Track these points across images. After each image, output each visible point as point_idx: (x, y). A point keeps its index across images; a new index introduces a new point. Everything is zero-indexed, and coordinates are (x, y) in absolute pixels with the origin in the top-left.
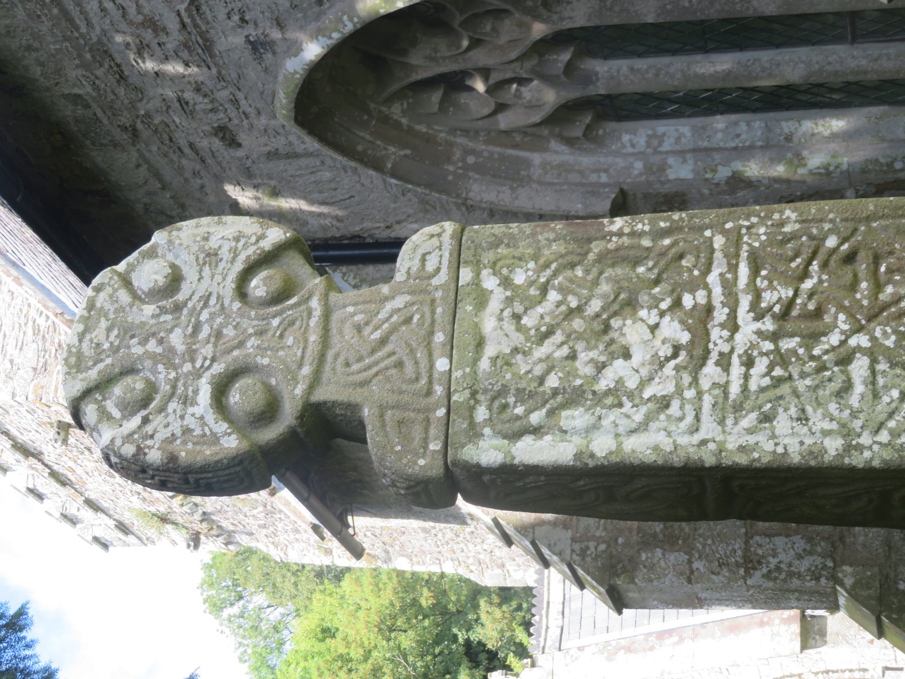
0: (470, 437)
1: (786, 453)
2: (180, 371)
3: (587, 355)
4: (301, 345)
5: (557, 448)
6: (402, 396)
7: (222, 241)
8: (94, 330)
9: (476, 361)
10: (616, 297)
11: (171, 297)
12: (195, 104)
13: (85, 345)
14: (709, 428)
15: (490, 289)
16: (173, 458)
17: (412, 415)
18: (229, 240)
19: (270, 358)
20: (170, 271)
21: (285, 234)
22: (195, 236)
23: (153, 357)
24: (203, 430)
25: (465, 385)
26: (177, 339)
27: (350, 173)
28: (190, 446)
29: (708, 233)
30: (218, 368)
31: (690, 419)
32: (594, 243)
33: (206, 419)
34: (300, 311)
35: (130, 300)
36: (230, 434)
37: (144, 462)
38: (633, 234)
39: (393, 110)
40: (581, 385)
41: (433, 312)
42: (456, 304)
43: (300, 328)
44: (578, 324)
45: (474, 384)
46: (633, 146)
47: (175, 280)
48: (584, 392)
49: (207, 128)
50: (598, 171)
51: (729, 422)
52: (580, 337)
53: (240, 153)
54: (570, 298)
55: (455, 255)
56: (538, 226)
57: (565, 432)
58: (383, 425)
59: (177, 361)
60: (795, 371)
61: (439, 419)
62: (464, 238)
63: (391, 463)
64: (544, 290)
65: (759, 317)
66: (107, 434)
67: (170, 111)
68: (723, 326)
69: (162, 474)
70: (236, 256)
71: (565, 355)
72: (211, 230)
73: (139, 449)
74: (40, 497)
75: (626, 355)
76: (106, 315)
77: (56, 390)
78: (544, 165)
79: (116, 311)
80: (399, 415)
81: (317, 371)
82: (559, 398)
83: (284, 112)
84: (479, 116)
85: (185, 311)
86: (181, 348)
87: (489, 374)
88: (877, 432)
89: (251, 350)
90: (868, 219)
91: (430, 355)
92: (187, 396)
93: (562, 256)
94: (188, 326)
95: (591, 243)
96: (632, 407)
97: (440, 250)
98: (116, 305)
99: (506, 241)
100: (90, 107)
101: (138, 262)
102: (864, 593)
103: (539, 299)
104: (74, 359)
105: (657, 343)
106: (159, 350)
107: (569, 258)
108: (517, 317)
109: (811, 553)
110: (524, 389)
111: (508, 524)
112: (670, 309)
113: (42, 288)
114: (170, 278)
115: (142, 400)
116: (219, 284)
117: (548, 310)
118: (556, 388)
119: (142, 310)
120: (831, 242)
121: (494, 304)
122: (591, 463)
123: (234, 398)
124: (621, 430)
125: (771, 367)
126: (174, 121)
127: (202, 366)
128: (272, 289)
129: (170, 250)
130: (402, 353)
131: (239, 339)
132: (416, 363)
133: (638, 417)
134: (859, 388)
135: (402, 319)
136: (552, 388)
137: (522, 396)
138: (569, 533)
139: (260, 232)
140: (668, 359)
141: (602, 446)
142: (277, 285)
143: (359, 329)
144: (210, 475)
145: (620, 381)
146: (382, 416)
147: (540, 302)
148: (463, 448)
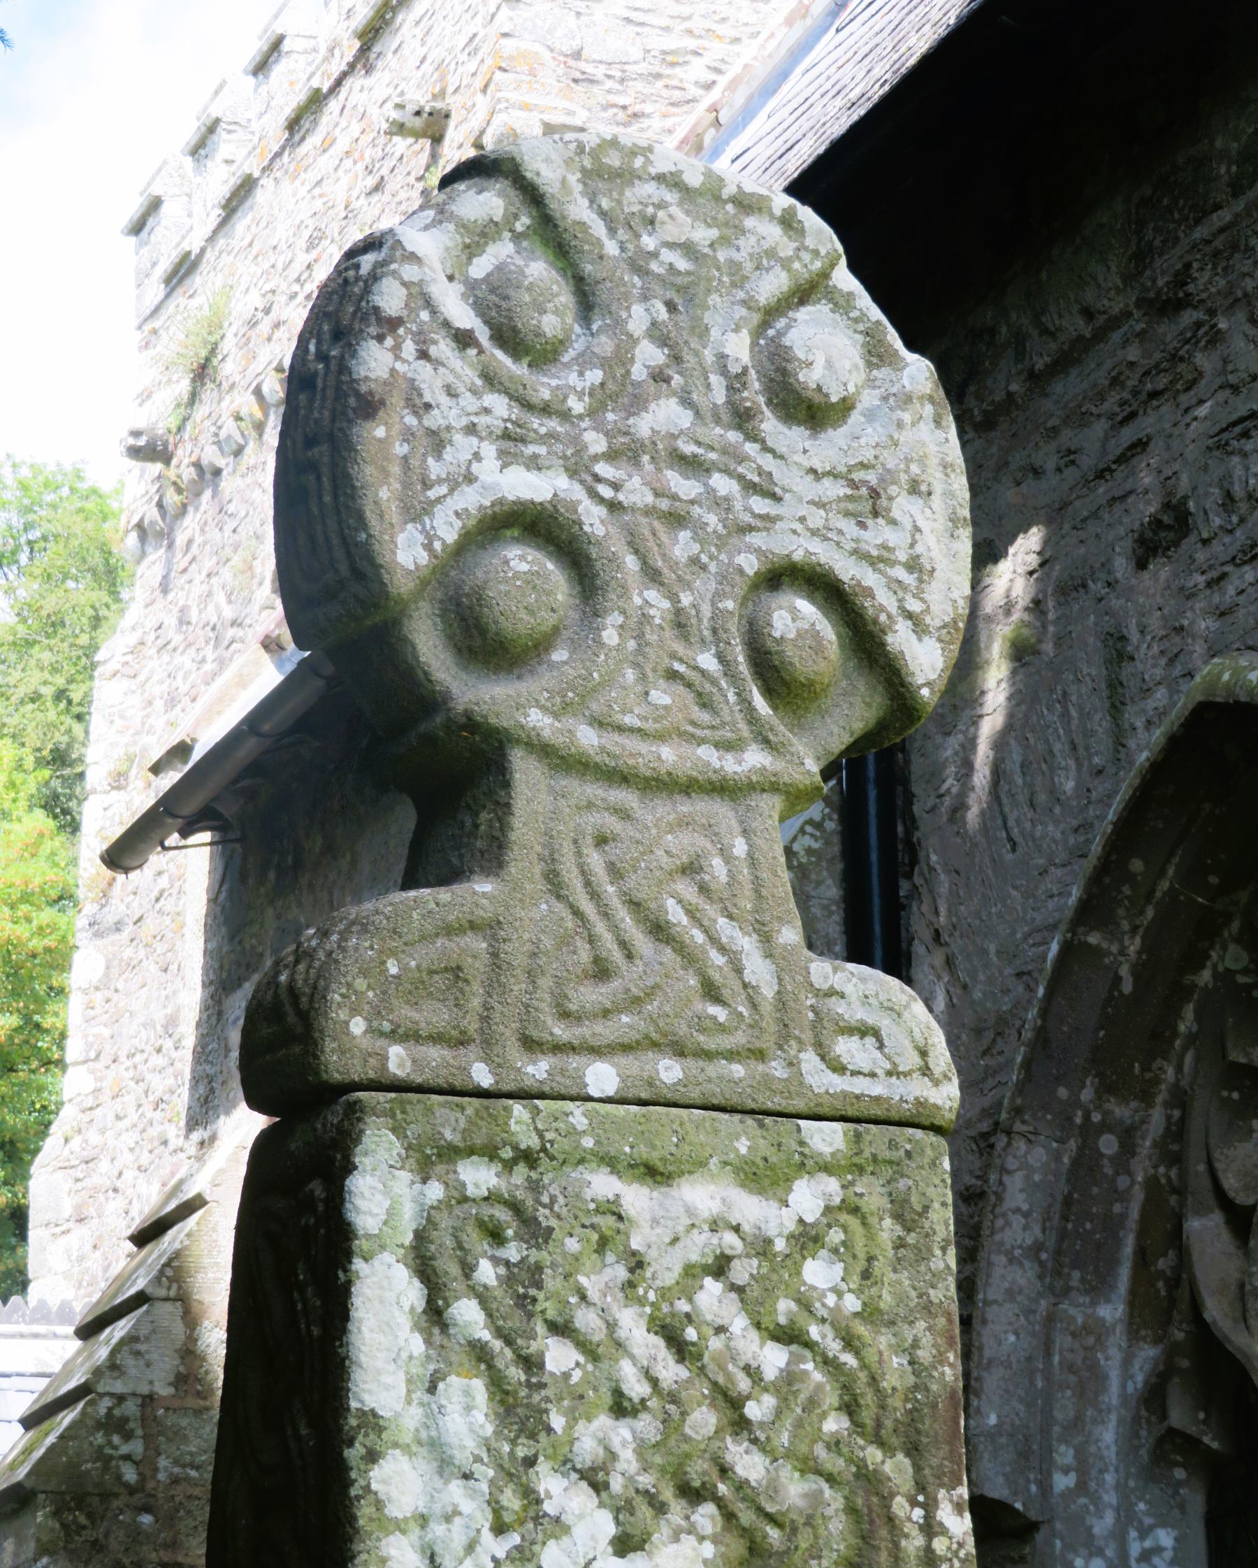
0: (420, 1149)
2: (586, 424)
3: (624, 1444)
4: (649, 726)
5: (392, 1367)
6: (523, 977)
7: (909, 526)
8: (688, 213)
9: (610, 1162)
10: (771, 1519)
11: (769, 403)
12: (1245, 455)
13: (649, 190)
15: (791, 1199)
16: (370, 407)
17: (476, 1003)
18: (912, 546)
19: (618, 648)
20: (834, 399)
21: (928, 684)
22: (922, 461)
23: (621, 359)
24: (440, 481)
25: (549, 1136)
26: (664, 416)
27: (1072, 841)
28: (400, 449)
30: (593, 519)
32: (907, 1461)
33: (466, 489)
34: (734, 723)
35: (762, 301)
36: (428, 547)
37: (360, 335)
39: (1233, 948)
40: (549, 1430)
41: (731, 1055)
42: (752, 1112)
43: (693, 723)
44: (703, 1420)
45: (552, 1158)
46: (1146, 1556)
47: (813, 413)
48: (533, 1436)
49: (1184, 484)
50: (1082, 1467)
53: (1122, 566)
54: (769, 1401)
55: (878, 1112)
56: (950, 1321)
57: (432, 1389)
58: (450, 931)
59: (610, 416)
61: (465, 1070)
62: (919, 1134)
63: (356, 949)
64: (788, 1336)
66: (430, 245)
67: (1228, 391)
69: (331, 381)
71: (625, 1389)
72: (936, 501)
73: (394, 324)
74: (261, 67)
76: (724, 241)
77: (525, 107)
78: (1095, 1331)
79: (735, 267)
80: (477, 968)
81: (586, 765)
82: (516, 1374)
83: (1226, 677)
84: (1217, 1165)
85: (733, 436)
86: (644, 425)
87: (578, 1196)
89: (638, 601)
92: (523, 440)
93: (874, 1380)
94: (699, 444)
95: (908, 1454)
96: (494, 1559)
97: (889, 1074)
98: (749, 266)
99: (911, 1239)
100: (1235, 195)
101: (856, 321)
103: (766, 1321)
104: (617, 164)
106: (638, 372)
107: (869, 1399)
108: (720, 1267)
110: (539, 1285)
111: (189, 1235)
113: (782, 75)
114: (817, 399)
115: (515, 330)
116: (802, 519)
117: (739, 1344)
118: (541, 1366)
119: (737, 330)
121: (752, 1210)
122: (354, 1454)
123: (520, 560)
124: (438, 1529)
126: (1201, 402)
127: (598, 479)
128: (790, 652)
129: (885, 399)
130: (630, 977)
131: (666, 571)
132: (606, 1013)
135: (717, 977)
136: (541, 1355)
137: (522, 1279)
139: (933, 621)
141: (395, 1481)
142: (803, 664)
143: (691, 869)
144: (327, 499)
145: (559, 1527)
146: (473, 926)
147: (758, 1326)
148: (393, 1130)
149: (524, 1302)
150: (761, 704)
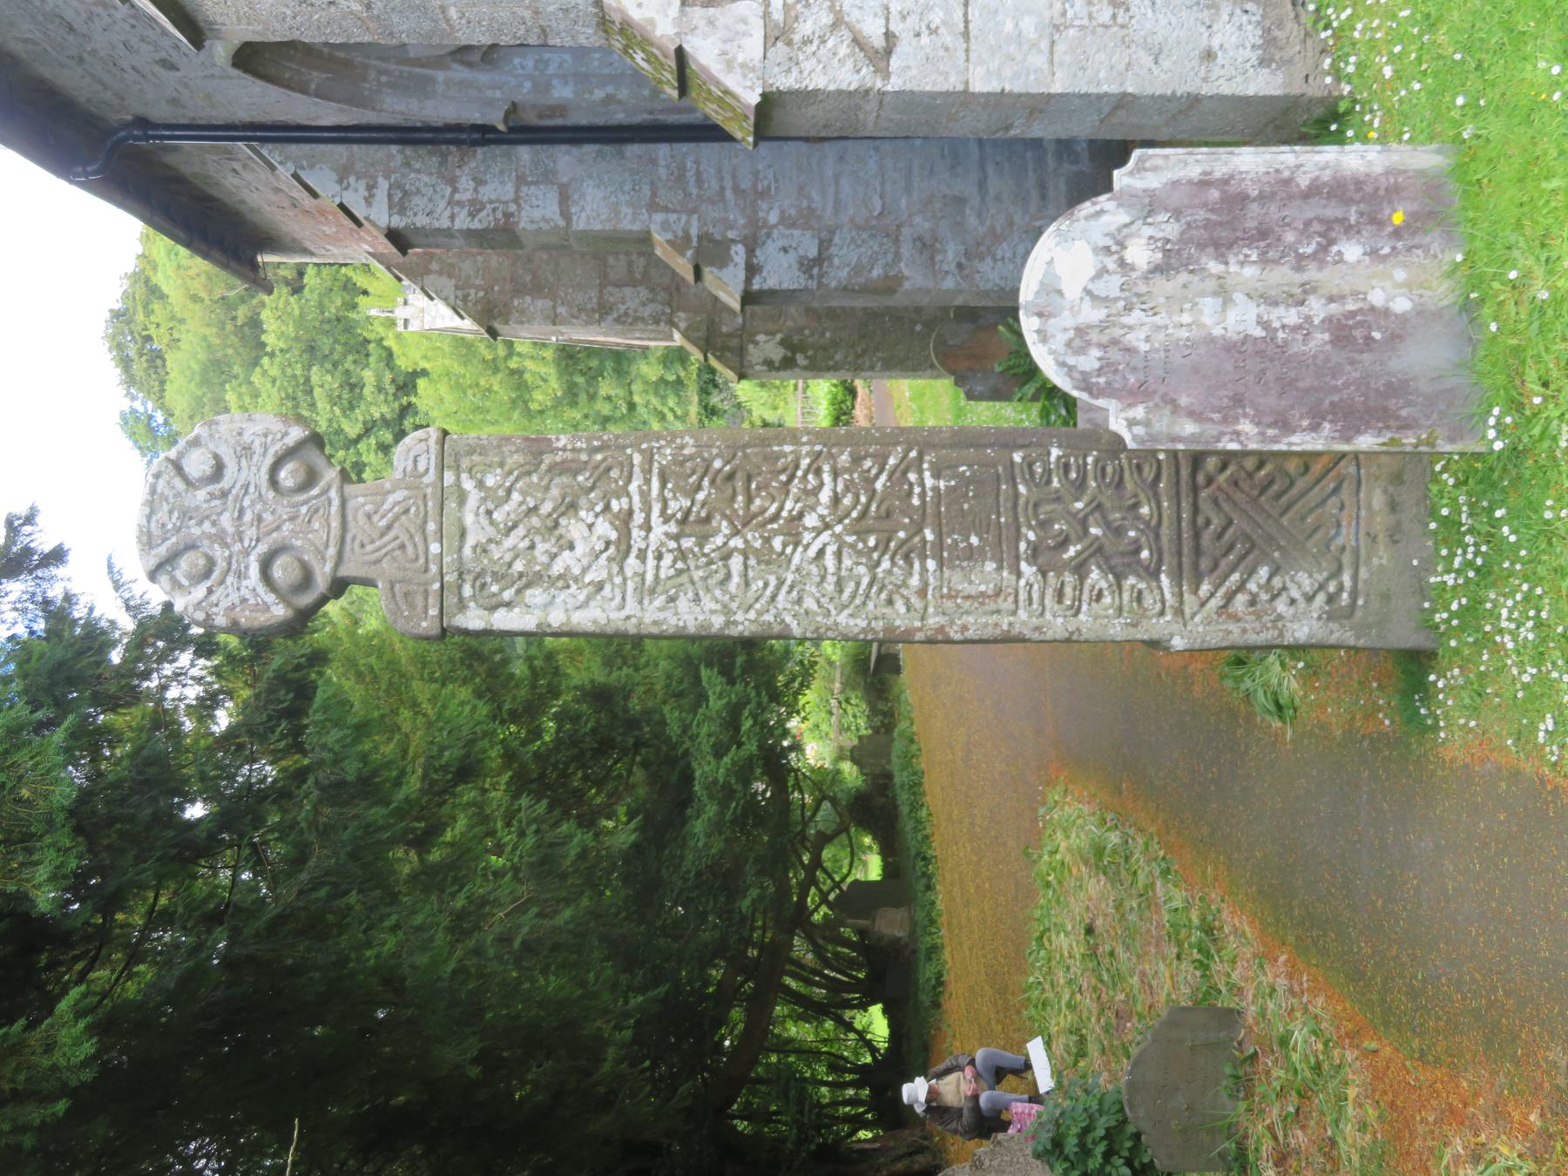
1: (685, 627)
13: (153, 525)
14: (631, 607)
23: (210, 537)
26: (226, 521)
29: (629, 451)
30: (263, 548)
31: (618, 599)
38: (574, 450)
44: (535, 521)
46: (523, 68)
51: (646, 602)
52: (538, 531)
58: (394, 596)
60: (692, 564)
64: (509, 491)
65: (666, 522)
68: (641, 527)
70: (266, 450)
73: (208, 615)
75: (571, 547)
76: (166, 500)
78: (447, 82)
79: (175, 496)
86: (231, 530)
88: (747, 611)
90: (744, 447)
91: (425, 540)
102: (696, 335)
105: (594, 539)
106: (213, 531)
108: (489, 513)
109: (652, 301)
112: (603, 511)
120: (717, 464)
123: (277, 572)
125: (675, 561)
130: (404, 538)
133: (582, 597)
134: (736, 579)
137: (497, 577)
138: (453, 282)
140: (602, 552)
141: (556, 619)
143: (369, 516)
145: (568, 568)
149: (503, 576)
150: (315, 492)
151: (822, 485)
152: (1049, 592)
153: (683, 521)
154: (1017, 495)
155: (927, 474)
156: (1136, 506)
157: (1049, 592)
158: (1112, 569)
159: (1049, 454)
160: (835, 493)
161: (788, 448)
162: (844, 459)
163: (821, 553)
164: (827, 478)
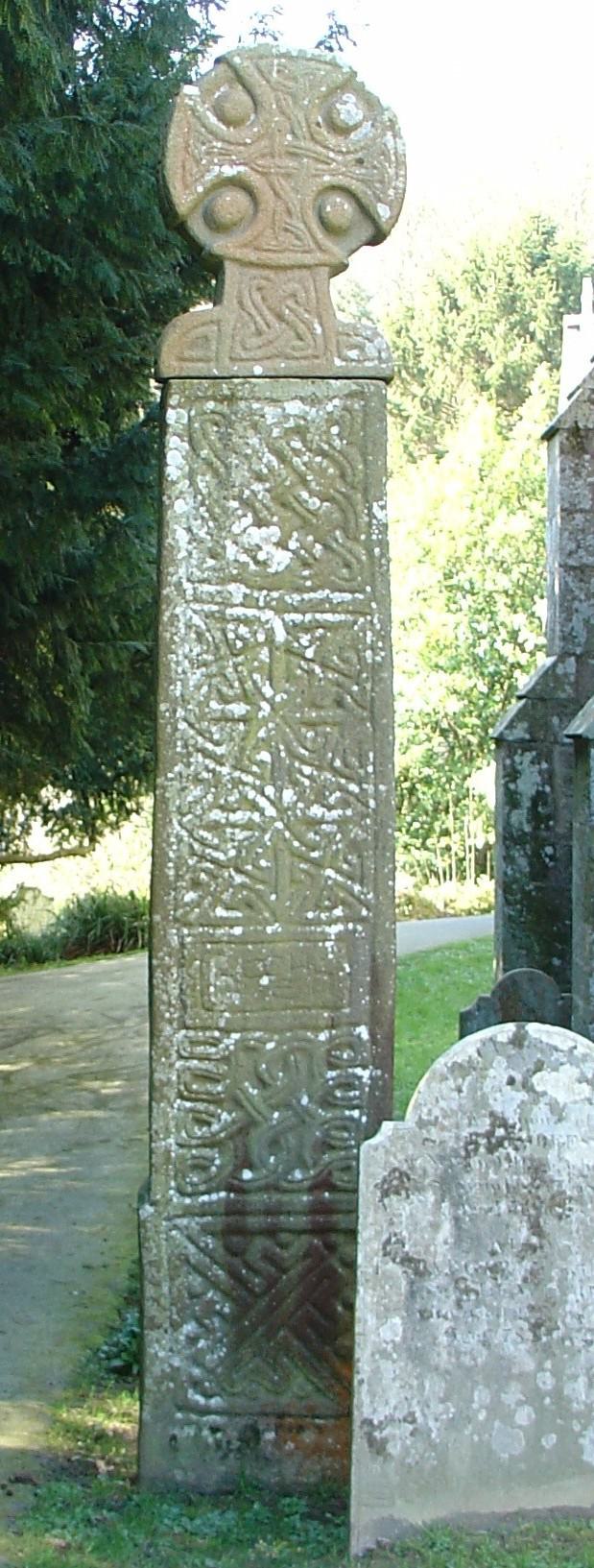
30: (255, 180)
38: (370, 524)
41: (305, 358)
47: (344, 131)
60: (240, 659)
133: (202, 534)
150: (320, 236)
151: (330, 808)
152: (205, 1065)
153: (289, 651)
154: (317, 1029)
155: (340, 927)
156: (304, 1167)
157: (205, 1065)
158: (231, 1137)
159: (365, 1067)
160: (322, 821)
161: (370, 769)
162: (356, 832)
163: (255, 806)
164: (335, 814)
